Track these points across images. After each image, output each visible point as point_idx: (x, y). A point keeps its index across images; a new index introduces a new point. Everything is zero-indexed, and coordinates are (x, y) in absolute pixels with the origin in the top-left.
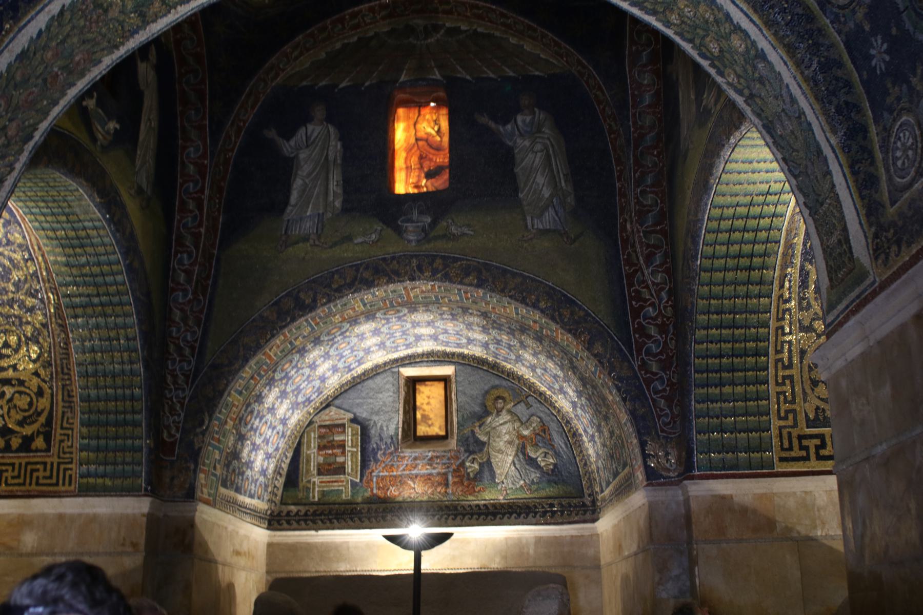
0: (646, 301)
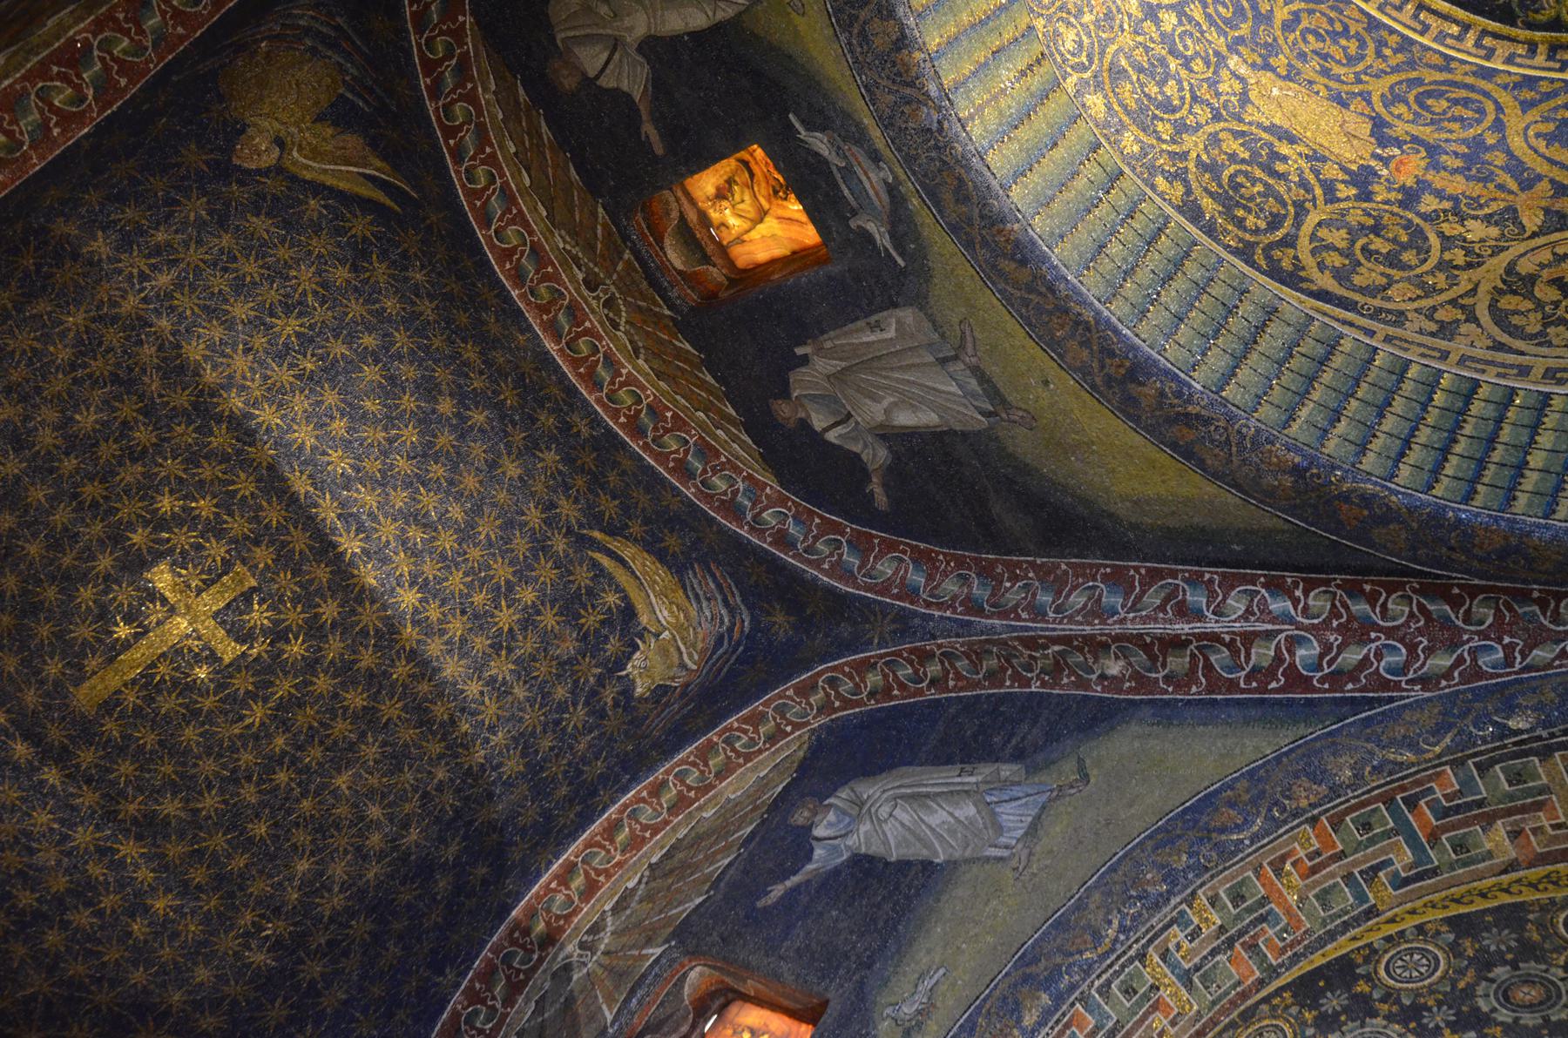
0: (1278, 658)
